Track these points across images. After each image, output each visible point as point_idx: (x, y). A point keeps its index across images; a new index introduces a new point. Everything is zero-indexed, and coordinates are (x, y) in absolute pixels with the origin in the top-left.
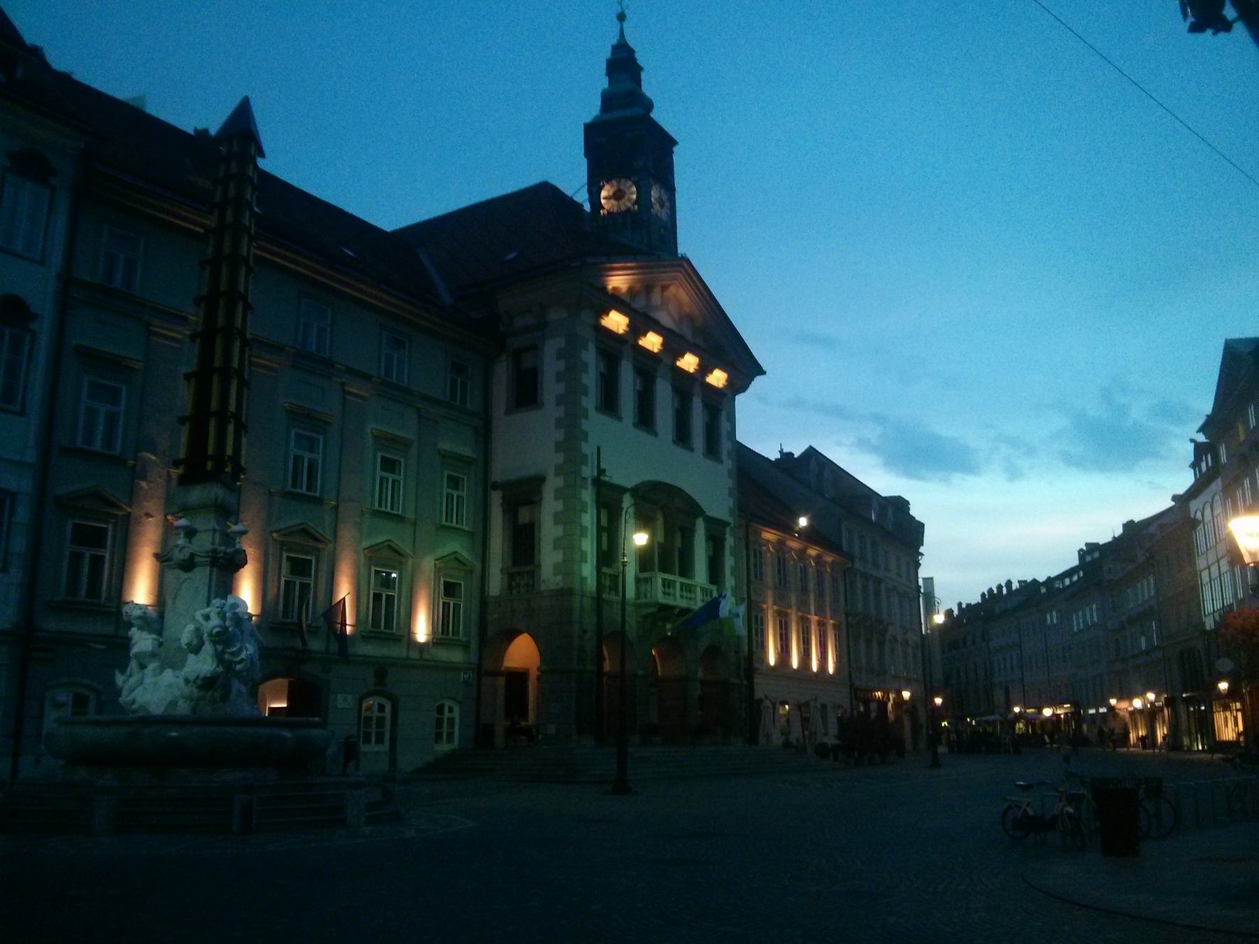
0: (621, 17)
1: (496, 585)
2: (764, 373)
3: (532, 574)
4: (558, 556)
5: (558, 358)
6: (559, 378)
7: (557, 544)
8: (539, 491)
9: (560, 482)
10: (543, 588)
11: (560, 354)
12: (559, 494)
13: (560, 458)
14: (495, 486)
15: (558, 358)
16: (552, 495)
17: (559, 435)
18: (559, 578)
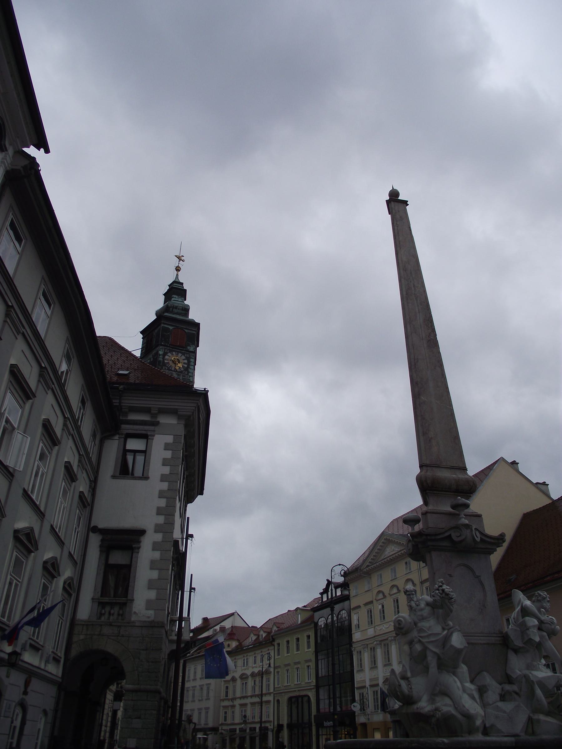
0: (178, 269)
1: (85, 610)
2: (202, 494)
3: (125, 604)
4: (152, 595)
5: (166, 449)
6: (165, 462)
7: (151, 585)
8: (139, 542)
9: (159, 537)
10: (133, 618)
11: (167, 447)
12: (156, 546)
13: (161, 519)
14: (95, 530)
15: (166, 449)
16: (150, 547)
17: (162, 503)
18: (151, 613)
